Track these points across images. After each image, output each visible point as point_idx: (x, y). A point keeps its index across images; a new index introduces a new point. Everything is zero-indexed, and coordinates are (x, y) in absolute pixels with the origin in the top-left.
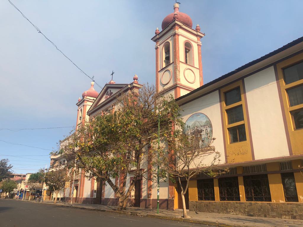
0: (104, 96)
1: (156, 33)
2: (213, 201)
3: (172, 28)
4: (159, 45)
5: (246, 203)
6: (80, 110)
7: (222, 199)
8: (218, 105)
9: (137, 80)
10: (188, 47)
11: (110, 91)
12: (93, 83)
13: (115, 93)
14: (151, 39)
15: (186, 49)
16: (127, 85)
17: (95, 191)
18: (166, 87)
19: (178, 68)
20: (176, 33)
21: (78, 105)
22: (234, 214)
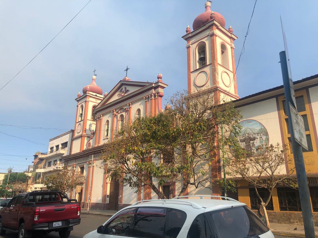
0: (117, 94)
1: (187, 31)
2: (273, 211)
3: (209, 28)
4: (191, 44)
5: (314, 214)
6: (80, 106)
7: (282, 208)
8: (276, 113)
9: (161, 79)
10: (223, 47)
11: (126, 88)
12: (94, 77)
13: (132, 92)
14: (182, 37)
15: (222, 51)
16: (152, 84)
17: (108, 196)
18: (203, 88)
19: (217, 70)
20: (214, 33)
21: (78, 101)
22: (299, 224)
